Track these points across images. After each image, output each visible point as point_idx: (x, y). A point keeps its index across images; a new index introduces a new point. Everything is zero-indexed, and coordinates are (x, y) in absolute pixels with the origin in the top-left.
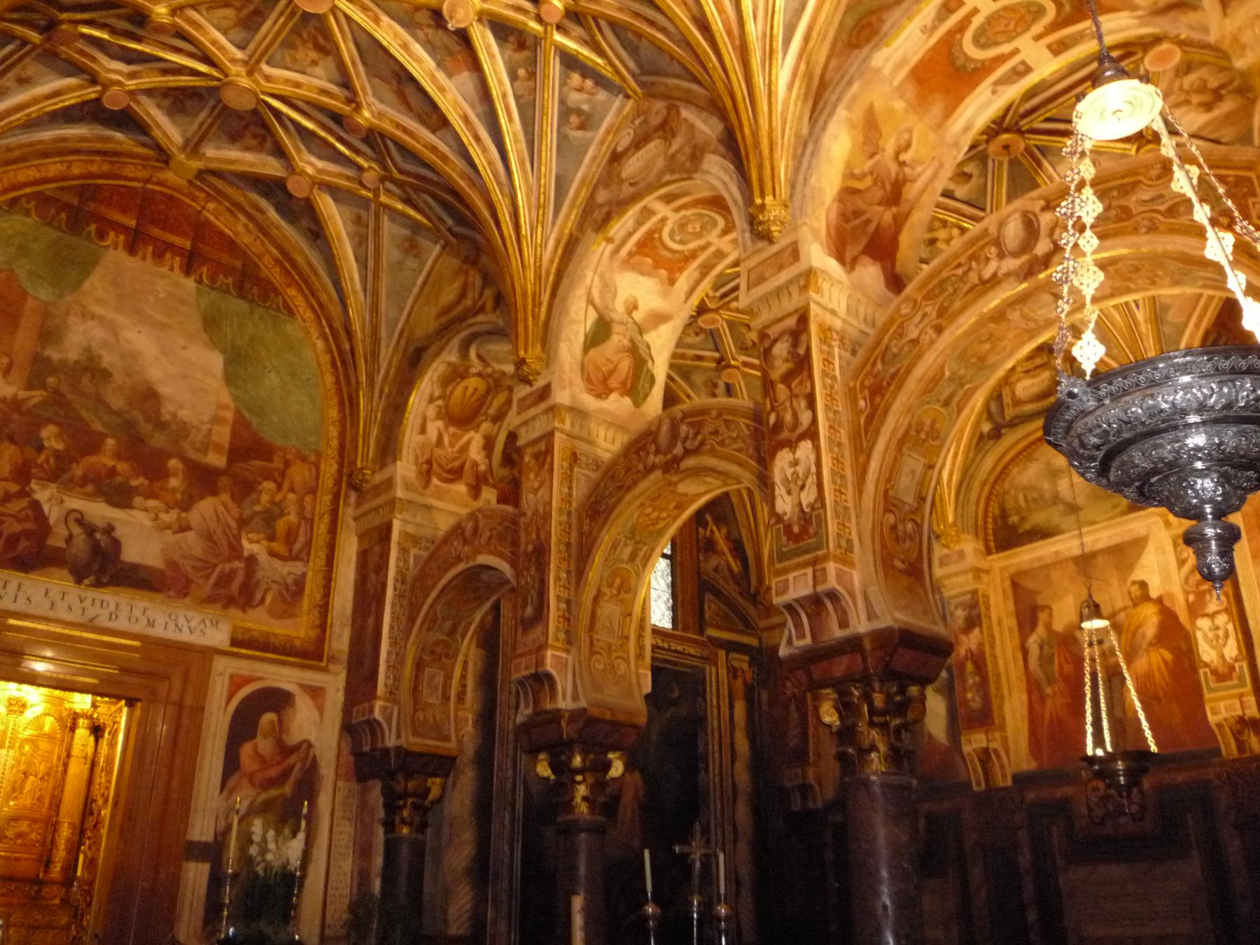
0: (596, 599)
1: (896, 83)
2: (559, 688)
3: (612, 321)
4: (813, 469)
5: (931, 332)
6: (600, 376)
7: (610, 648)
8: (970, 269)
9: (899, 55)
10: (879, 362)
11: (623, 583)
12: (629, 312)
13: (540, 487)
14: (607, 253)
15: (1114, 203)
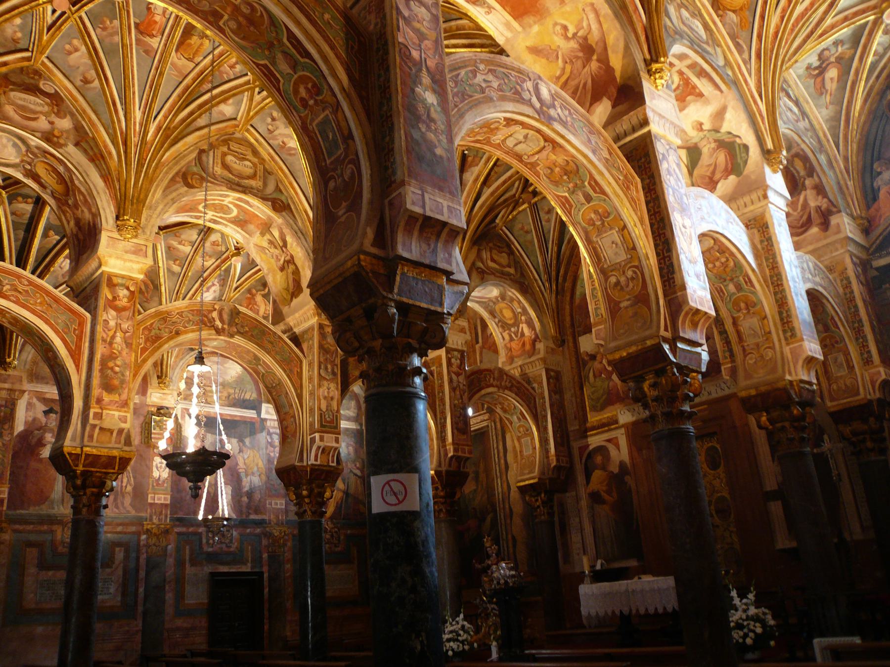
0: (735, 323)
1: (519, 29)
3: (696, 144)
6: (707, 180)
9: (501, 28)
11: (747, 305)
12: (701, 130)
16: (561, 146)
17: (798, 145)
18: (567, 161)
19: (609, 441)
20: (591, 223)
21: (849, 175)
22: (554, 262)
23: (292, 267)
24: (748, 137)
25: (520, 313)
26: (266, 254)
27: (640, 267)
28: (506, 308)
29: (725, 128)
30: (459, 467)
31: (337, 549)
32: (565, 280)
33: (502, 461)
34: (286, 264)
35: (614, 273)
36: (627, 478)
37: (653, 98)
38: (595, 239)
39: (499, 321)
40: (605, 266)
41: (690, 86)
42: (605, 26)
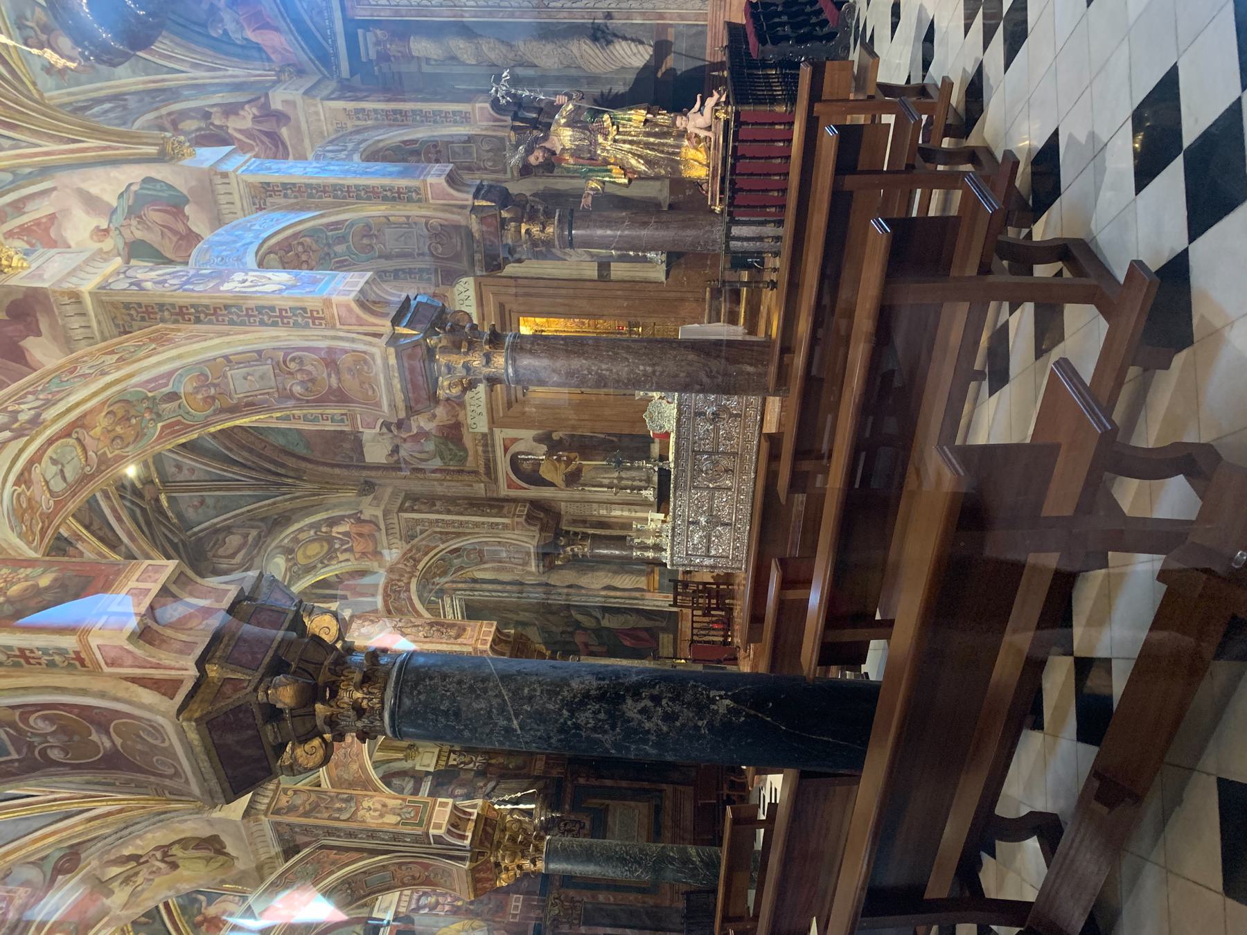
0: (388, 257)
3: (126, 243)
6: (183, 243)
11: (365, 236)
12: (106, 231)
16: (84, 416)
17: (161, 117)
19: (506, 450)
21: (220, 69)
22: (254, 474)
23: (175, 850)
24: (134, 174)
25: (315, 533)
26: (143, 890)
28: (306, 548)
29: (115, 204)
30: (506, 642)
31: (587, 826)
32: (283, 465)
33: (508, 587)
34: (166, 859)
36: (556, 436)
37: (40, 277)
38: (235, 401)
39: (322, 563)
41: (34, 228)
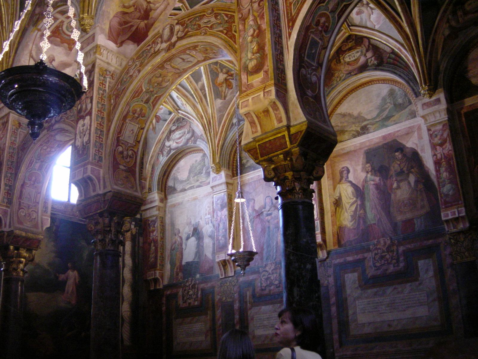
0: (23, 186)
2: (3, 222)
4: (89, 128)
5: (137, 72)
7: (29, 206)
8: (152, 47)
10: (120, 84)
11: (36, 179)
13: (3, 137)
14: (38, 36)
15: (197, 23)
18: (169, 81)
20: (134, 112)
27: (136, 153)
35: (123, 145)
38: (127, 121)
40: (121, 138)
42: (161, 17)
